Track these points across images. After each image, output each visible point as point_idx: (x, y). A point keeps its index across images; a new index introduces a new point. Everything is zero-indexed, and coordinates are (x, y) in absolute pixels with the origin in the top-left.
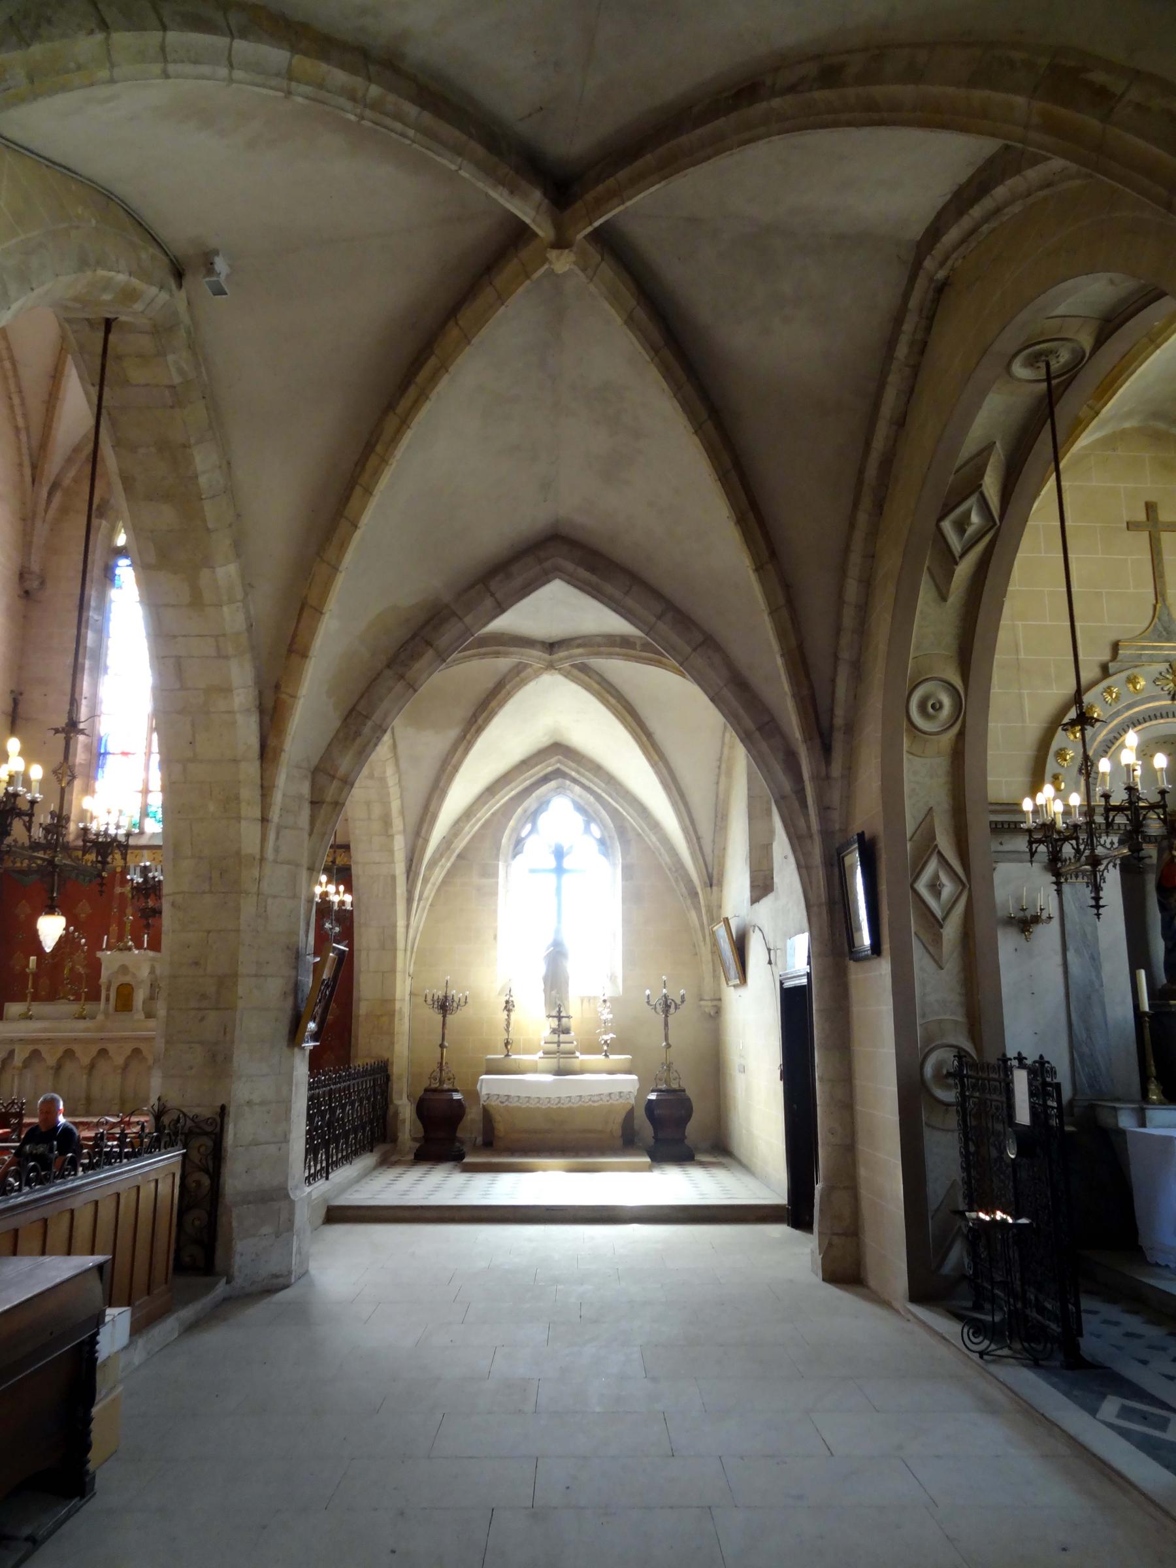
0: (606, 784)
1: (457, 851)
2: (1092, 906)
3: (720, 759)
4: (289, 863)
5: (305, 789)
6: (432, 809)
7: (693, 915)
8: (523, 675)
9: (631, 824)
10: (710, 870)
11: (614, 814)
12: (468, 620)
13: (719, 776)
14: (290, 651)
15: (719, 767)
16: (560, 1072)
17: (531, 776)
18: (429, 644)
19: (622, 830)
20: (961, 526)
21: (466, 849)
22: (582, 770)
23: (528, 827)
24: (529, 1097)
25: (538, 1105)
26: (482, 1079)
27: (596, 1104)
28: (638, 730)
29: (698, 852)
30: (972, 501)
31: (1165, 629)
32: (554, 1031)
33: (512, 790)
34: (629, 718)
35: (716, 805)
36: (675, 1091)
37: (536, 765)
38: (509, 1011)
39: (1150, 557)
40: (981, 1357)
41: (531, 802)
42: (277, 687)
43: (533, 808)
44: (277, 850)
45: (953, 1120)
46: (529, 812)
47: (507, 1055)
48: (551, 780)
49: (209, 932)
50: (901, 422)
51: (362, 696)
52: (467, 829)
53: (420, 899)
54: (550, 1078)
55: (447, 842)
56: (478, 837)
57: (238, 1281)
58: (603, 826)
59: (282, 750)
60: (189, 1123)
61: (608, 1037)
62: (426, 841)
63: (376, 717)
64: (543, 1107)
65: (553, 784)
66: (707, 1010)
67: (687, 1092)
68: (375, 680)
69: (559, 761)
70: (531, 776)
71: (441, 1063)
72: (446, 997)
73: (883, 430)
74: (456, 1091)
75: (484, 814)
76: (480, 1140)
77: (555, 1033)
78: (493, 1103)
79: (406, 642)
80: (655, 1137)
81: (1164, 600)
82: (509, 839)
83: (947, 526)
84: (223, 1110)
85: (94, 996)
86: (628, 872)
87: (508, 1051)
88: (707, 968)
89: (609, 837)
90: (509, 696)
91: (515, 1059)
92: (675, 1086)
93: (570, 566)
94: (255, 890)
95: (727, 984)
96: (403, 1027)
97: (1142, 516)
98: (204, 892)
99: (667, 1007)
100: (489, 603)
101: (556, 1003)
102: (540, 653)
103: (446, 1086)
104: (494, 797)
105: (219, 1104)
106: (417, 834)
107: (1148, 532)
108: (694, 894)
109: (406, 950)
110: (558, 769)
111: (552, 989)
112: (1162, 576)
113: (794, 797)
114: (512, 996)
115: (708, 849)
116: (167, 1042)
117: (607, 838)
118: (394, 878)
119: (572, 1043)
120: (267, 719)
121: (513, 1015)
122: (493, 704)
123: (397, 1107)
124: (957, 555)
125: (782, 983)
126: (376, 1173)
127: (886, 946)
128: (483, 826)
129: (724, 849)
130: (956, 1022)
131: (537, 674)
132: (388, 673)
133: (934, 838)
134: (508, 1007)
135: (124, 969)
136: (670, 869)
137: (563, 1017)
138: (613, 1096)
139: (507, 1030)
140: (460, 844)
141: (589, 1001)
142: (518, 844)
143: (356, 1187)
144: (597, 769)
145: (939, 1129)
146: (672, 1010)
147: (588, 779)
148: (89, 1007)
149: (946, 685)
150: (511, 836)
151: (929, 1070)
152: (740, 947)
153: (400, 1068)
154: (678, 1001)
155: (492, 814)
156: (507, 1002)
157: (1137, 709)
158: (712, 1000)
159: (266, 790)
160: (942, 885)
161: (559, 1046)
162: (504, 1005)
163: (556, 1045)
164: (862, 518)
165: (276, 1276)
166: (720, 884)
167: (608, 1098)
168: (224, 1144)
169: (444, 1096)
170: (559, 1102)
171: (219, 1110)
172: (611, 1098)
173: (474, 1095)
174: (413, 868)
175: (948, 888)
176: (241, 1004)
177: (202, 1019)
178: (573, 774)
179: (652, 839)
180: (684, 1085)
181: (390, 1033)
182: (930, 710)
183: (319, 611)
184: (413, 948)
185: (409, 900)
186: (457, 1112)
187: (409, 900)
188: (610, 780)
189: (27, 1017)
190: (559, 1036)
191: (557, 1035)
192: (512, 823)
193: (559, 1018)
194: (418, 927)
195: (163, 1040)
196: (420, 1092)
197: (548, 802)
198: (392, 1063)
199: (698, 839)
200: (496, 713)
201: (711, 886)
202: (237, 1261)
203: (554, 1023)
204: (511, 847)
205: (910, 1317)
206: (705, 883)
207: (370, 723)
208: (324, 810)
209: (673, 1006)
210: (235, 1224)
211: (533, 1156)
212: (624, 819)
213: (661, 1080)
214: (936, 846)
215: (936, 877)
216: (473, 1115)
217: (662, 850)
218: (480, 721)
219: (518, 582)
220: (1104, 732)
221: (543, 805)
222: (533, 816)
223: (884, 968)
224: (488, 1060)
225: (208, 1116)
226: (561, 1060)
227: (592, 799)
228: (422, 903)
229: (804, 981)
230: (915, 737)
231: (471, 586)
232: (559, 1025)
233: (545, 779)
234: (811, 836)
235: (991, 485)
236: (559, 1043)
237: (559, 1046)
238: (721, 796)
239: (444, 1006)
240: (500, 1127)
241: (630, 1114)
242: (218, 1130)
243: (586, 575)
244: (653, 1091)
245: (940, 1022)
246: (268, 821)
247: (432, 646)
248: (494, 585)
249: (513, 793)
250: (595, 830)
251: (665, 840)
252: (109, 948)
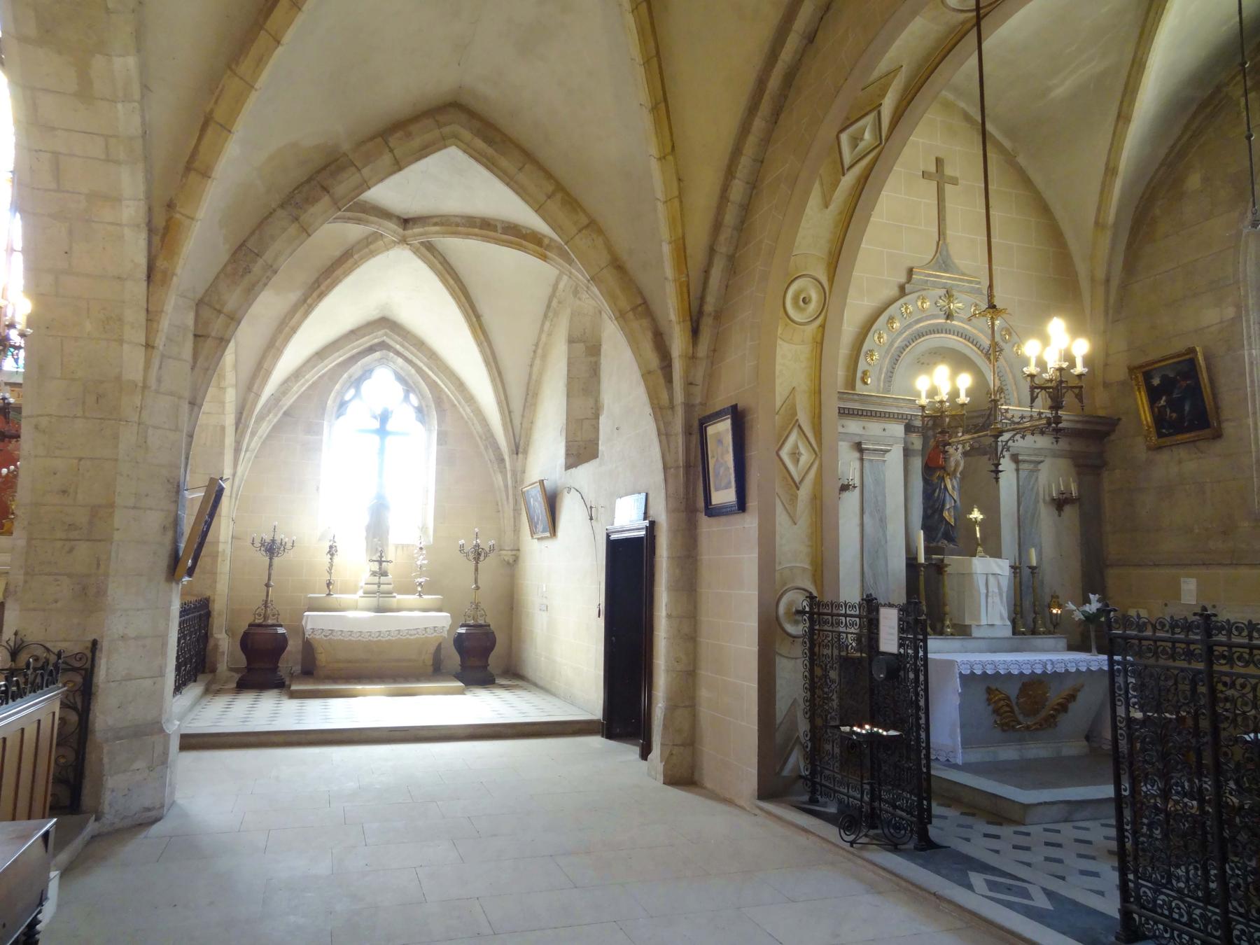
0: (428, 359)
1: (285, 408)
2: (992, 471)
3: (537, 345)
4: (171, 394)
5: (190, 320)
6: (265, 366)
7: (498, 480)
8: (372, 247)
9: (448, 396)
10: (517, 440)
11: (433, 386)
12: (366, 171)
13: (533, 359)
14: (188, 168)
15: (535, 352)
16: (380, 609)
17: (359, 346)
18: (325, 189)
19: (439, 400)
20: (855, 141)
21: (291, 407)
22: (406, 344)
23: (352, 392)
24: (352, 631)
25: (360, 638)
26: (308, 616)
27: (412, 637)
28: (470, 311)
29: (509, 424)
30: (869, 120)
31: (944, 263)
32: (374, 574)
33: (340, 357)
34: (463, 299)
35: (528, 384)
36: (481, 626)
37: (364, 336)
38: (332, 555)
39: (937, 202)
40: (852, 846)
41: (356, 369)
42: (170, 206)
43: (356, 376)
44: (159, 381)
45: (799, 650)
46: (353, 379)
47: (329, 594)
48: (376, 351)
49: (81, 459)
50: (811, 38)
51: (253, 233)
52: (295, 388)
53: (246, 451)
54: (373, 614)
55: (276, 399)
56: (304, 397)
57: (109, 817)
58: (421, 396)
59: (173, 274)
62: (258, 396)
63: (269, 255)
64: (364, 640)
65: (377, 355)
66: (506, 559)
67: (491, 627)
68: (266, 218)
69: (386, 334)
70: (359, 346)
71: (266, 601)
72: (273, 541)
73: (793, 42)
74: (281, 626)
75: (311, 376)
76: (297, 669)
77: (375, 576)
78: (317, 637)
79: (302, 184)
80: (463, 665)
81: (945, 239)
82: (334, 402)
83: (844, 137)
84: (95, 643)
86: (442, 438)
87: (330, 591)
89: (427, 406)
90: (356, 265)
91: (336, 598)
92: (482, 622)
93: (467, 135)
94: (136, 419)
95: (532, 537)
96: (224, 567)
97: (933, 169)
98: (75, 417)
100: (387, 159)
101: (377, 549)
102: (396, 227)
103: (270, 622)
104: (323, 361)
105: (91, 638)
106: (249, 388)
107: (936, 182)
108: (501, 460)
109: (231, 497)
110: (383, 341)
111: (374, 537)
112: (944, 220)
113: (659, 372)
114: (335, 542)
115: (517, 422)
116: (26, 574)
117: (424, 406)
118: (223, 428)
119: (390, 584)
120: (157, 239)
121: (336, 559)
122: (339, 272)
123: (218, 640)
124: (846, 165)
125: (608, 536)
126: (204, 702)
127: (752, 503)
128: (310, 387)
129: (532, 423)
130: (804, 569)
131: (387, 248)
132: (281, 213)
133: (795, 414)
134: (332, 551)
136: (481, 437)
137: (384, 561)
138: (428, 630)
139: (330, 573)
140: (288, 402)
141: (403, 548)
142: (343, 405)
143: (191, 716)
144: (420, 345)
145: (784, 656)
146: (482, 558)
147: (412, 353)
149: (814, 281)
150: (336, 398)
152: (552, 502)
153: (219, 606)
154: (488, 549)
155: (320, 377)
156: (331, 547)
157: (921, 325)
158: (512, 550)
159: (152, 316)
160: (800, 454)
161: (379, 587)
162: (328, 549)
163: (376, 586)
164: (759, 124)
165: (149, 810)
166: (526, 452)
167: (424, 632)
168: (95, 680)
169: (270, 631)
170: (379, 636)
171: (89, 645)
172: (426, 632)
173: (300, 631)
174: (243, 421)
175: (805, 457)
176: (117, 536)
177: (71, 550)
178: (398, 347)
179: (466, 411)
180: (489, 621)
182: (801, 303)
183: (227, 129)
184: (237, 495)
185: (237, 450)
186: (280, 644)
187: (237, 450)
188: (433, 356)
190: (380, 578)
191: (378, 577)
192: (338, 387)
193: (380, 562)
194: (243, 476)
195: (22, 572)
196: (244, 627)
197: (371, 371)
198: (214, 601)
199: (510, 412)
200: (340, 281)
201: (517, 454)
202: (107, 797)
203: (375, 567)
204: (335, 409)
205: (758, 811)
206: (512, 450)
207: (260, 262)
208: (209, 344)
209: (483, 554)
210: (106, 760)
211: (356, 684)
212: (441, 390)
213: (469, 617)
214: (797, 420)
215: (796, 447)
216: (293, 646)
217: (475, 422)
218: (323, 288)
219: (416, 143)
220: (899, 340)
221: (367, 374)
222: (357, 382)
223: (749, 523)
224: (310, 598)
225: (77, 651)
226: (381, 599)
227: (413, 371)
228: (248, 453)
229: (643, 533)
230: (786, 325)
231: (372, 138)
232: (380, 568)
233: (371, 350)
234: (672, 407)
235: (888, 105)
236: (379, 584)
237: (379, 587)
238: (534, 377)
239: (272, 549)
240: (322, 658)
241: (439, 648)
242: (88, 665)
243: (480, 144)
244: (462, 626)
245: (791, 568)
246: (153, 347)
247: (328, 192)
248: (393, 141)
249: (341, 359)
250: (414, 399)
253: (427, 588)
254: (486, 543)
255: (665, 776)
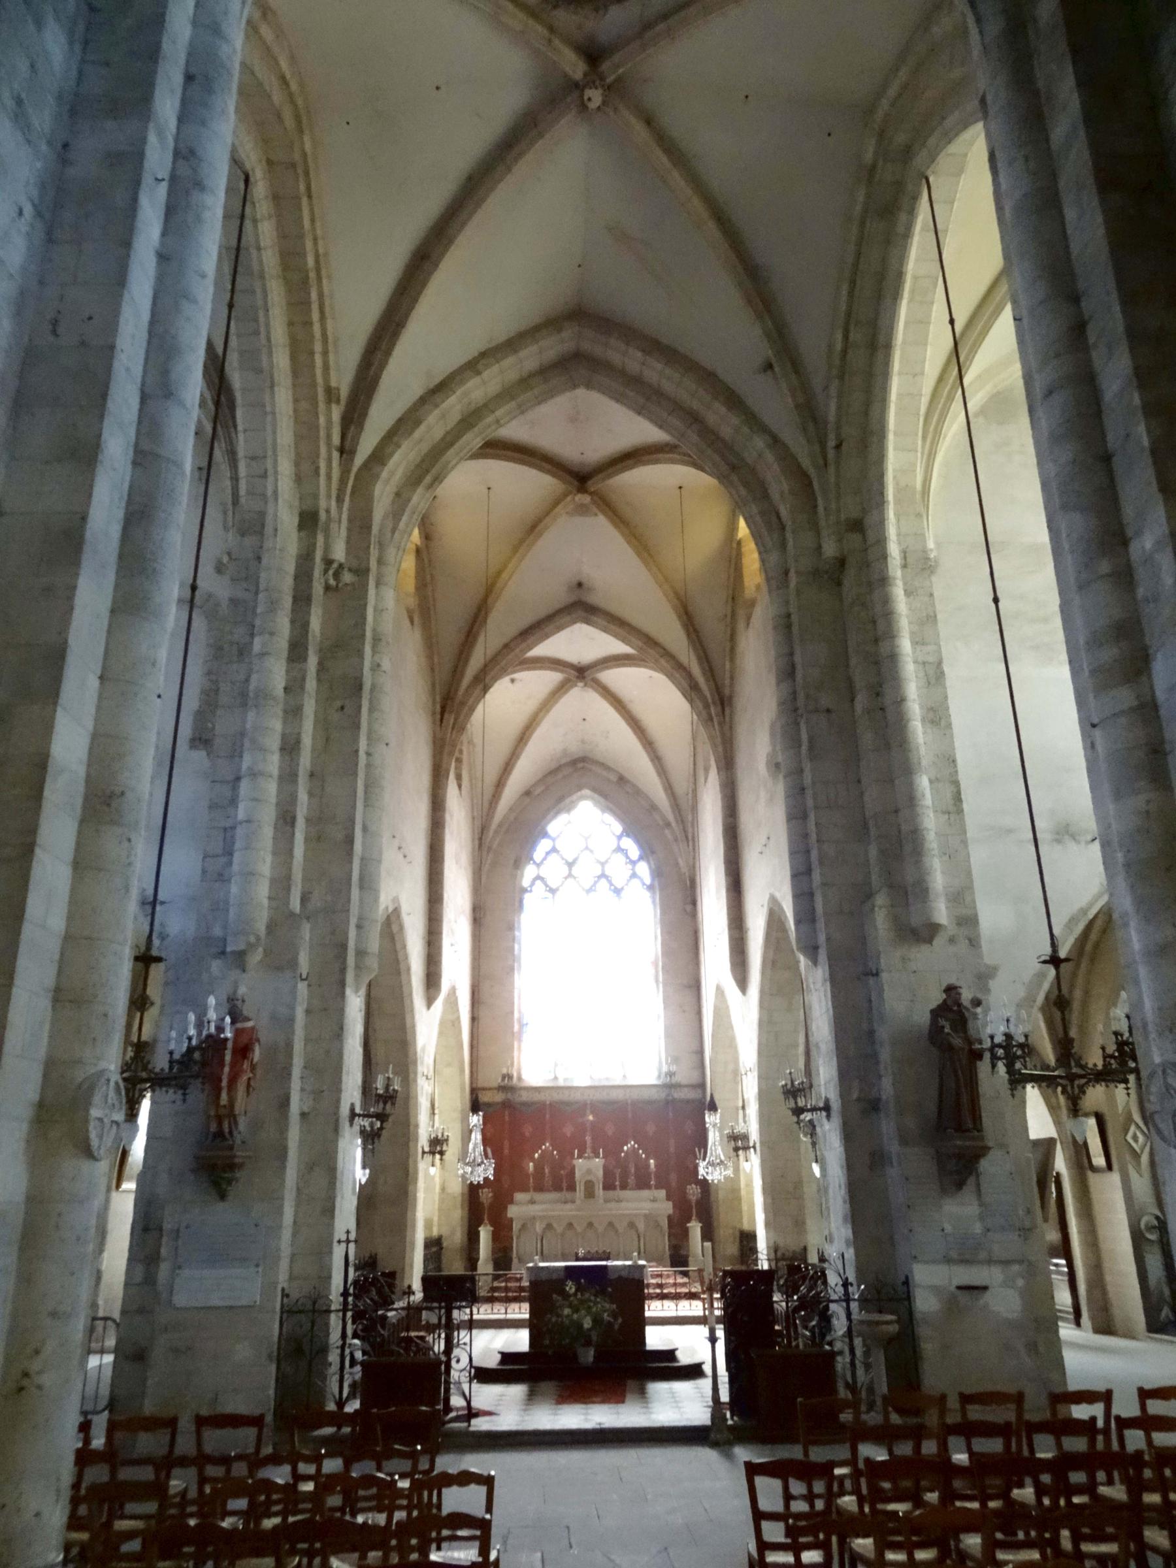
60: (791, 1255)
84: (805, 1249)
85: (572, 1188)
105: (802, 1245)
127: (1115, 1166)
135: (589, 1171)
148: (568, 1195)
151: (1143, 1226)
175: (1141, 1138)
181: (741, 1212)
189: (532, 1202)
223: (1115, 1178)
252: (580, 1157)
255: (1093, 1328)
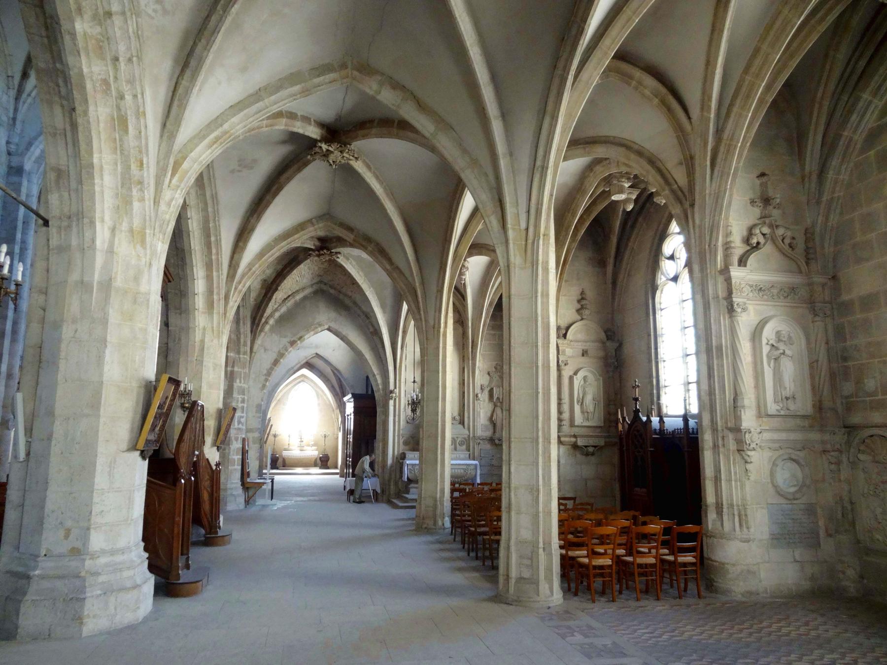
7: (333, 415)
11: (316, 391)
61: (313, 443)
88: (336, 428)
99: (325, 437)
108: (334, 411)
173: (281, 456)
233: (300, 382)
239: (275, 436)
241: (316, 460)
251: (328, 398)
253: (313, 445)
254: (327, 434)
